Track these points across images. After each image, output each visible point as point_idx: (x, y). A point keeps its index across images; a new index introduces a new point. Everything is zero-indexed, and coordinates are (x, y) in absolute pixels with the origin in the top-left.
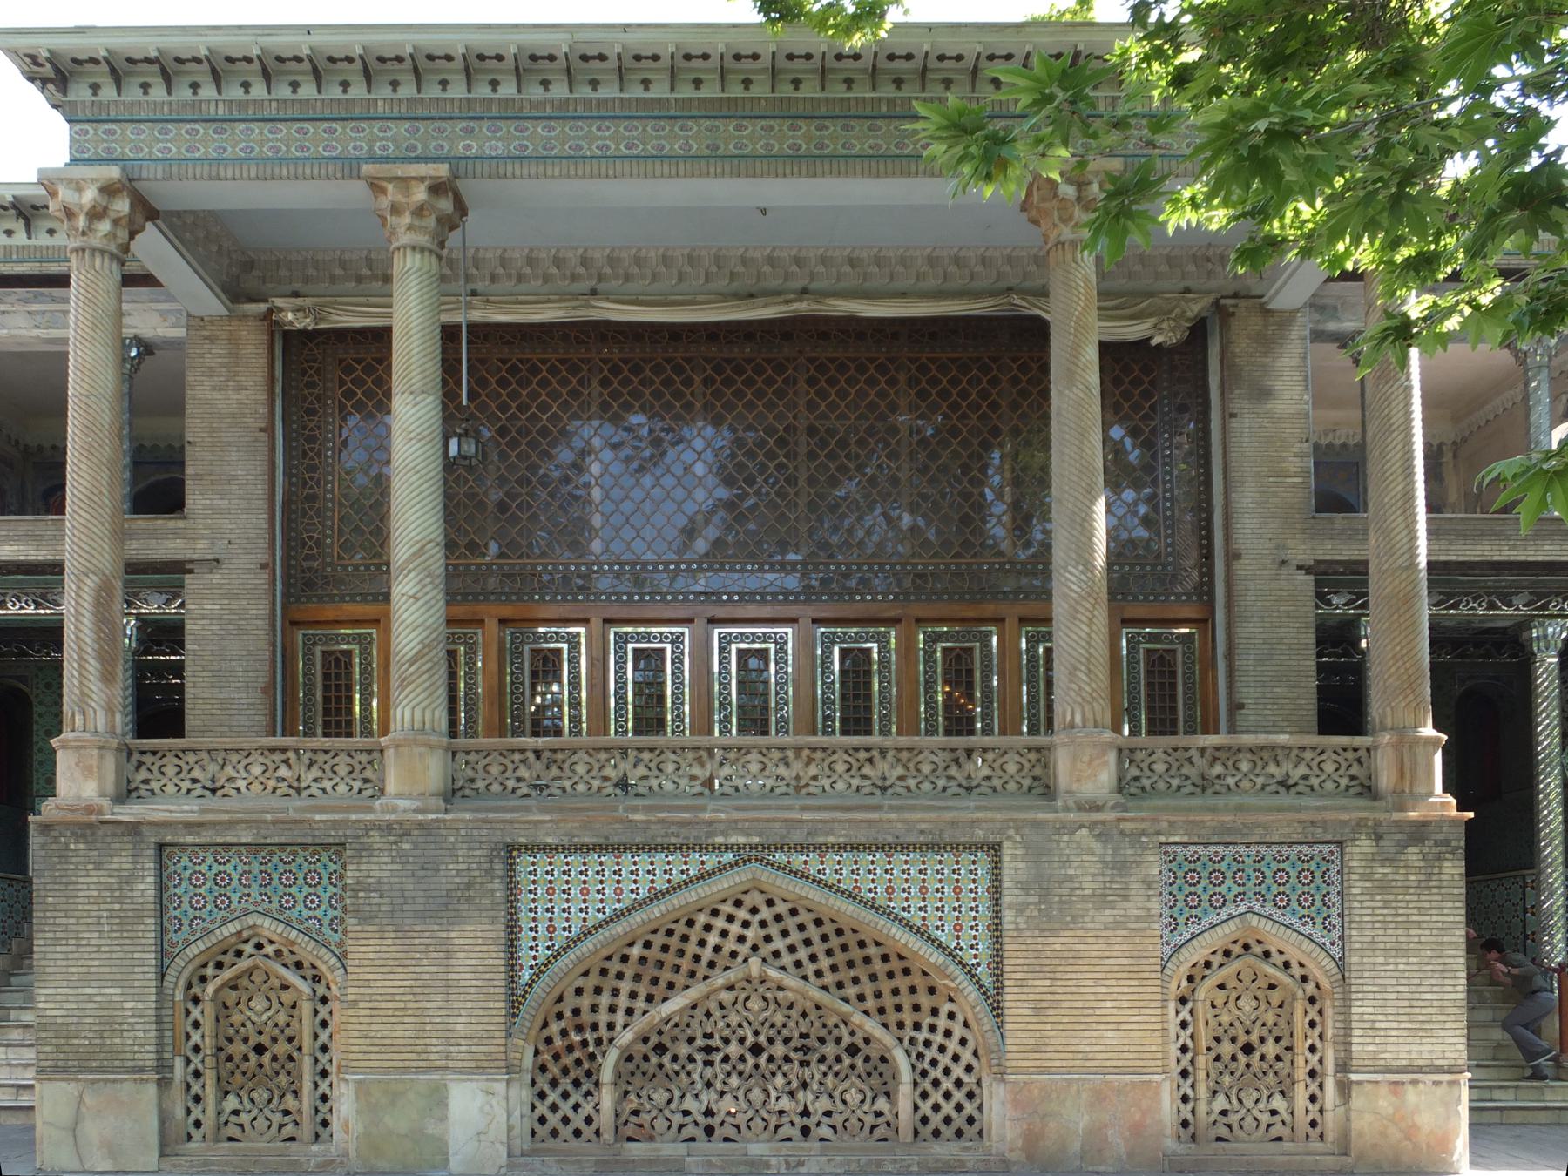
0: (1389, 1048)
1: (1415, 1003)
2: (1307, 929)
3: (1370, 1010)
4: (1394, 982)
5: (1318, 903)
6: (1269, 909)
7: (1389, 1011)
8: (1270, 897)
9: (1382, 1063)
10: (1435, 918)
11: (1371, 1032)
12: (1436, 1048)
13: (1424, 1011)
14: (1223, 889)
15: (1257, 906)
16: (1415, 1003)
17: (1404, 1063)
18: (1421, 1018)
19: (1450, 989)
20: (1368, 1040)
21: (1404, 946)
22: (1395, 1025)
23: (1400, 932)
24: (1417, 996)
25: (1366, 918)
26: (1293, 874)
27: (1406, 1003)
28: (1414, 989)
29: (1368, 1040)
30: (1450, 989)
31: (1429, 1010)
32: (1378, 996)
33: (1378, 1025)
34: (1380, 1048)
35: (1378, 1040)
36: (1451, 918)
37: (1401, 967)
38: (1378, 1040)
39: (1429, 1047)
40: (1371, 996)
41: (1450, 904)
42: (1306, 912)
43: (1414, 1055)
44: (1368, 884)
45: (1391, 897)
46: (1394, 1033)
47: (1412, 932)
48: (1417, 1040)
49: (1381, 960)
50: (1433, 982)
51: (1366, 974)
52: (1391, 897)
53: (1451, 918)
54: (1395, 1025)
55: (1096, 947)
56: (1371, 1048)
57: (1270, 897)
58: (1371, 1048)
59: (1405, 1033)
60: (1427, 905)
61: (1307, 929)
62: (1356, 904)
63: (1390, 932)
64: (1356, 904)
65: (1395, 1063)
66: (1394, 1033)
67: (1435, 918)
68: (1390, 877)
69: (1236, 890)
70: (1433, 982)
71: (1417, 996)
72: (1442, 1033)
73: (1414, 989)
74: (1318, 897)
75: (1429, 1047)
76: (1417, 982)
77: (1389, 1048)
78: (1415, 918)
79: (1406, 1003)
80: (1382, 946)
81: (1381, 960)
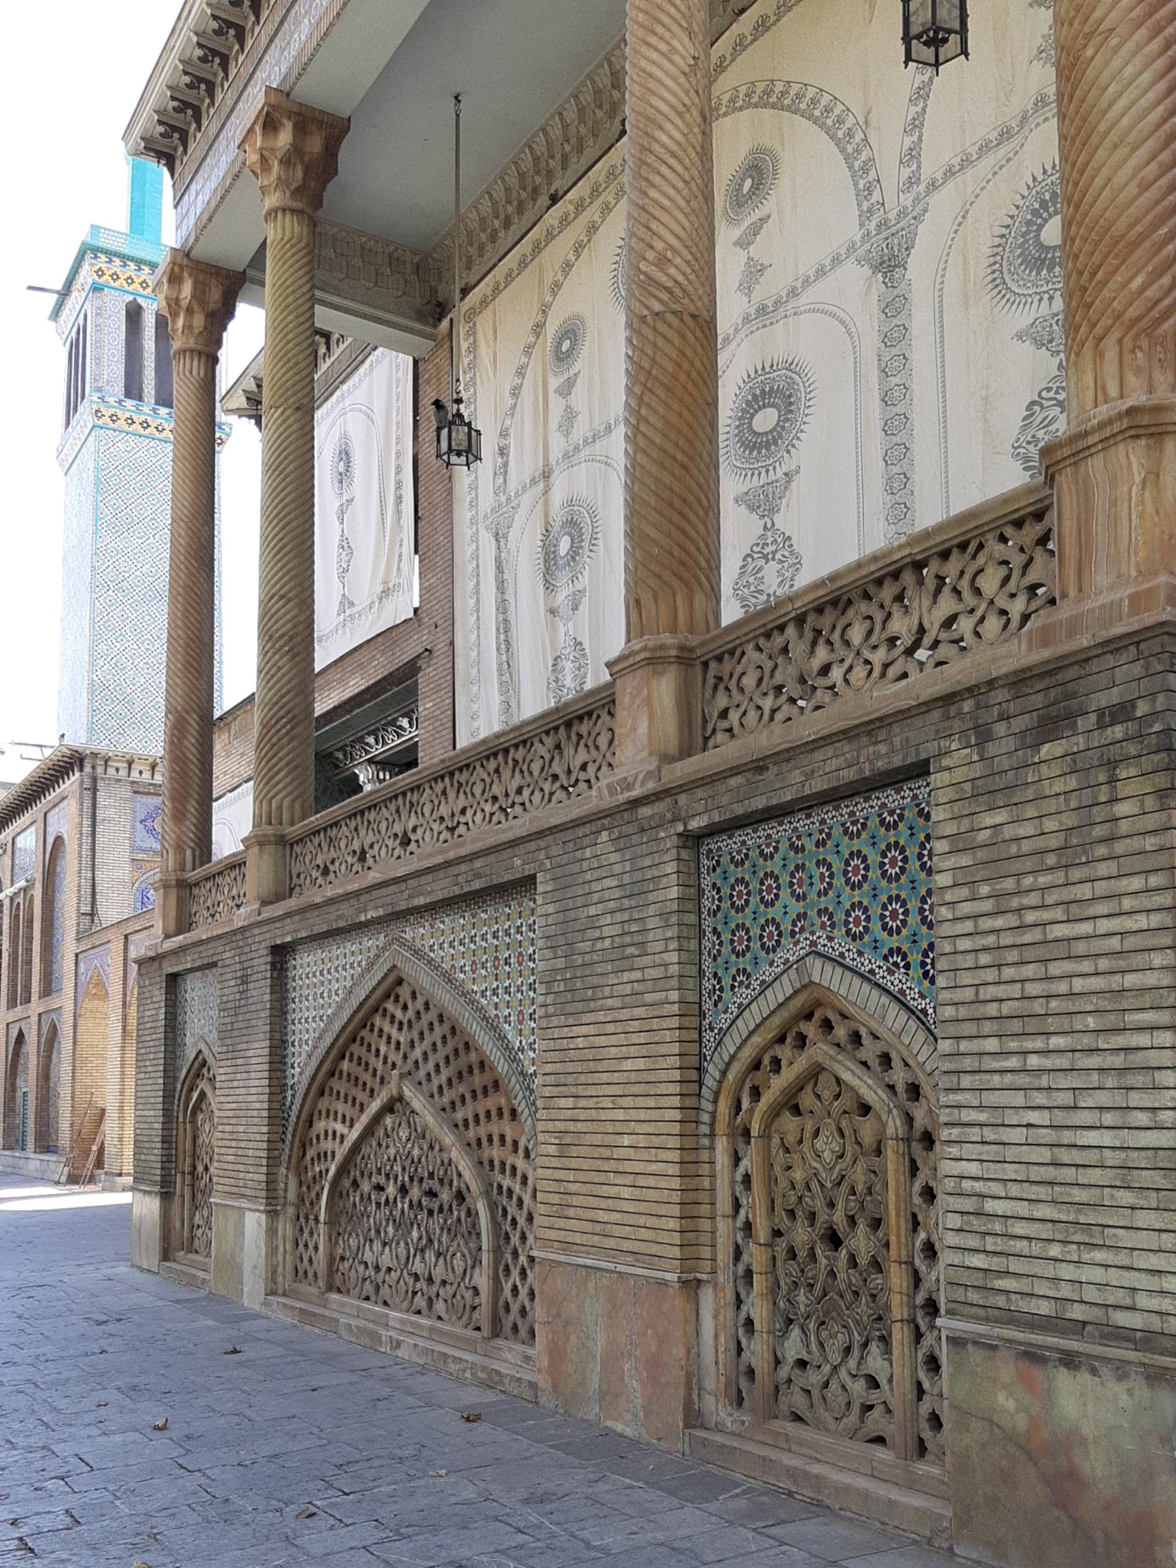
0: (1015, 1266)
1: (1065, 1156)
2: (895, 981)
3: (973, 1168)
4: (1019, 1099)
5: (914, 919)
6: (840, 945)
7: (1010, 1171)
8: (840, 916)
9: (1001, 1301)
10: (1104, 926)
11: (976, 1223)
12: (1114, 1277)
13: (1084, 1177)
14: (775, 912)
15: (821, 937)
16: (1065, 1156)
17: (1045, 1308)
18: (1080, 1195)
19: (1142, 1118)
20: (972, 1241)
21: (1038, 1007)
22: (1023, 1209)
23: (1029, 971)
24: (1067, 1137)
25: (964, 944)
26: (873, 858)
27: (1045, 1155)
28: (1060, 1117)
29: (972, 1241)
30: (1142, 1118)
31: (1095, 1176)
32: (989, 1134)
33: (990, 1206)
34: (996, 1263)
35: (990, 1243)
36: (1142, 922)
37: (1033, 1061)
38: (990, 1243)
39: (1098, 1275)
40: (975, 1134)
41: (1136, 883)
42: (894, 941)
43: (1066, 1291)
44: (965, 860)
45: (1009, 884)
46: (1020, 1228)
47: (1056, 969)
48: (1073, 1252)
49: (992, 1045)
50: (1103, 1099)
51: (966, 1081)
52: (1009, 884)
53: (1142, 922)
54: (1023, 1209)
55: (613, 1040)
56: (978, 1261)
57: (840, 916)
58: (978, 1261)
59: (1045, 1231)
60: (1085, 891)
61: (895, 981)
62: (944, 912)
63: (1008, 973)
64: (944, 912)
65: (1025, 1305)
66: (1020, 1228)
67: (1104, 926)
68: (1008, 832)
69: (796, 908)
70: (1103, 1099)
71: (1067, 1137)
72: (1127, 1239)
73: (1060, 1117)
74: (913, 905)
75: (1098, 1275)
76: (1065, 1098)
77: (1015, 1266)
78: (1059, 931)
79: (1045, 1155)
80: (992, 1009)
81: (992, 1045)
